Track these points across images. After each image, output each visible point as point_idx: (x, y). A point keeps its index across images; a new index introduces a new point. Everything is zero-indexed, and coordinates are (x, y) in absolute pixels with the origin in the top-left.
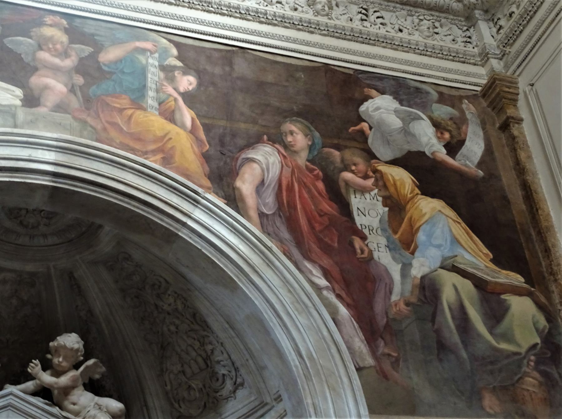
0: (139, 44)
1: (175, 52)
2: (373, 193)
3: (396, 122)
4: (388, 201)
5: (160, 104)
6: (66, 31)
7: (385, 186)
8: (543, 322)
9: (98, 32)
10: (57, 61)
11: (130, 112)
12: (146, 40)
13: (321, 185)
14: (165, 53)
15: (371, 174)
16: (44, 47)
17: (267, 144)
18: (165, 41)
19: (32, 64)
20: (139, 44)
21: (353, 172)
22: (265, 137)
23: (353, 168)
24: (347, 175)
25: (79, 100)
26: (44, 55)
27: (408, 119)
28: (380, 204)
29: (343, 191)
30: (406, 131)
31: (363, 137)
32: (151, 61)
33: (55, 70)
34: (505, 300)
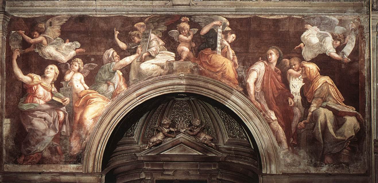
0: (215, 23)
1: (228, 23)
2: (299, 78)
3: (315, 40)
4: (305, 80)
5: (222, 50)
6: (189, 23)
7: (305, 74)
8: (358, 126)
9: (200, 21)
10: (185, 38)
11: (211, 56)
12: (217, 20)
13: (279, 77)
14: (224, 25)
15: (301, 68)
16: (181, 33)
17: (261, 61)
18: (225, 19)
19: (178, 41)
20: (215, 23)
21: (293, 69)
22: (260, 58)
23: (294, 67)
24: (291, 71)
25: (194, 55)
26: (181, 36)
27: (322, 38)
28: (302, 81)
29: (288, 78)
30: (321, 44)
31: (300, 49)
32: (219, 30)
33: (186, 41)
34: (345, 118)
